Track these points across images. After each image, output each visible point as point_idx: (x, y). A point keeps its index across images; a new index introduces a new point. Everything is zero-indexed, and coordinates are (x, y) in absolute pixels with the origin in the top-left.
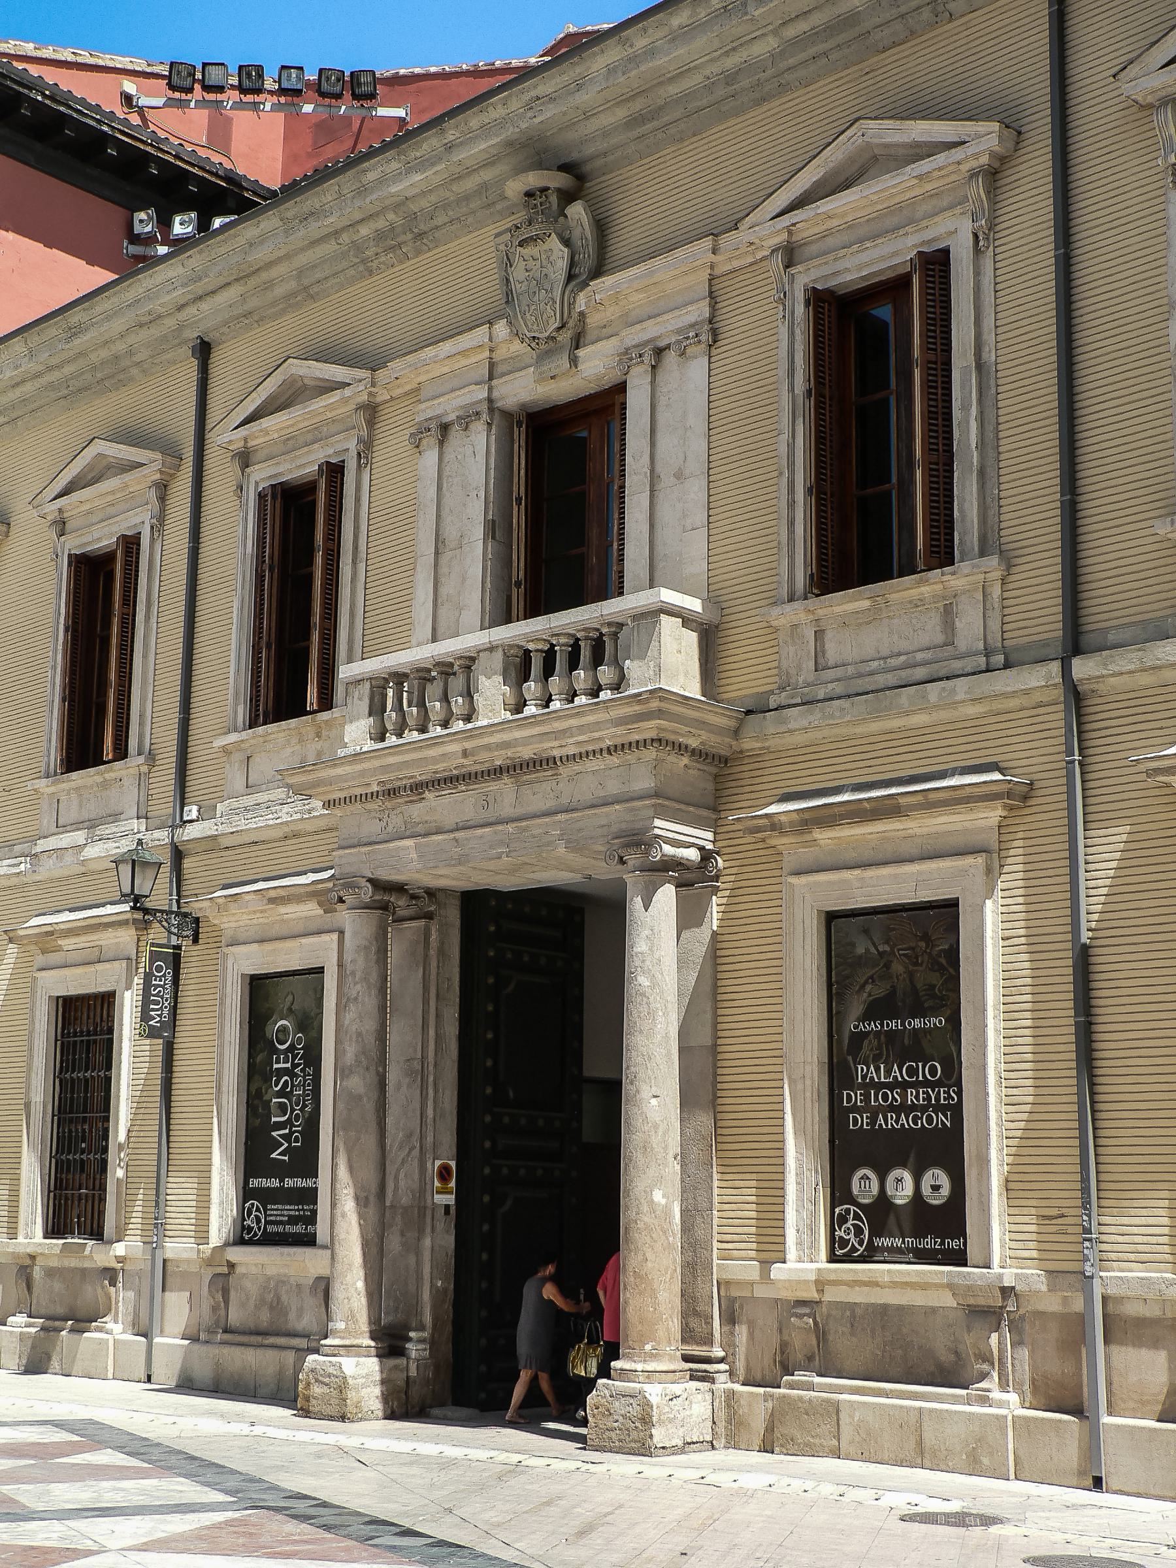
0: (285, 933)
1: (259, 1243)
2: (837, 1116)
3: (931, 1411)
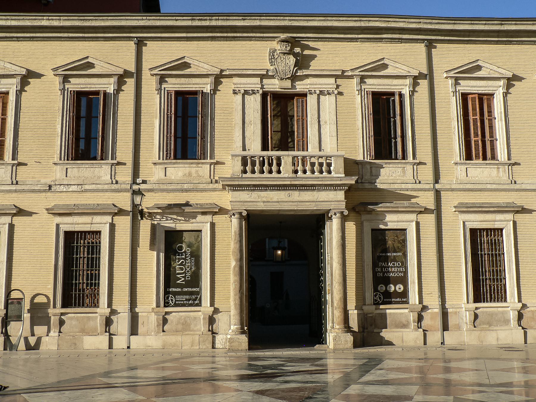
1: (172, 306)
2: (375, 273)
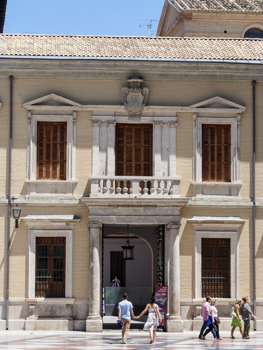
0: (50, 228)
3: (226, 321)
